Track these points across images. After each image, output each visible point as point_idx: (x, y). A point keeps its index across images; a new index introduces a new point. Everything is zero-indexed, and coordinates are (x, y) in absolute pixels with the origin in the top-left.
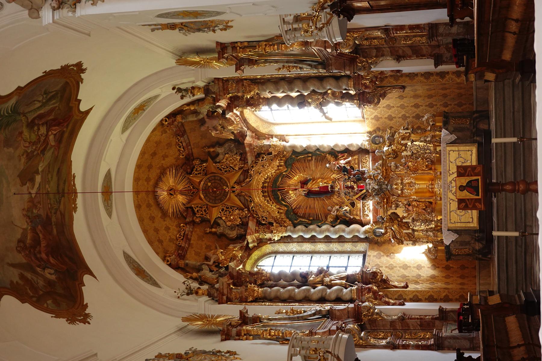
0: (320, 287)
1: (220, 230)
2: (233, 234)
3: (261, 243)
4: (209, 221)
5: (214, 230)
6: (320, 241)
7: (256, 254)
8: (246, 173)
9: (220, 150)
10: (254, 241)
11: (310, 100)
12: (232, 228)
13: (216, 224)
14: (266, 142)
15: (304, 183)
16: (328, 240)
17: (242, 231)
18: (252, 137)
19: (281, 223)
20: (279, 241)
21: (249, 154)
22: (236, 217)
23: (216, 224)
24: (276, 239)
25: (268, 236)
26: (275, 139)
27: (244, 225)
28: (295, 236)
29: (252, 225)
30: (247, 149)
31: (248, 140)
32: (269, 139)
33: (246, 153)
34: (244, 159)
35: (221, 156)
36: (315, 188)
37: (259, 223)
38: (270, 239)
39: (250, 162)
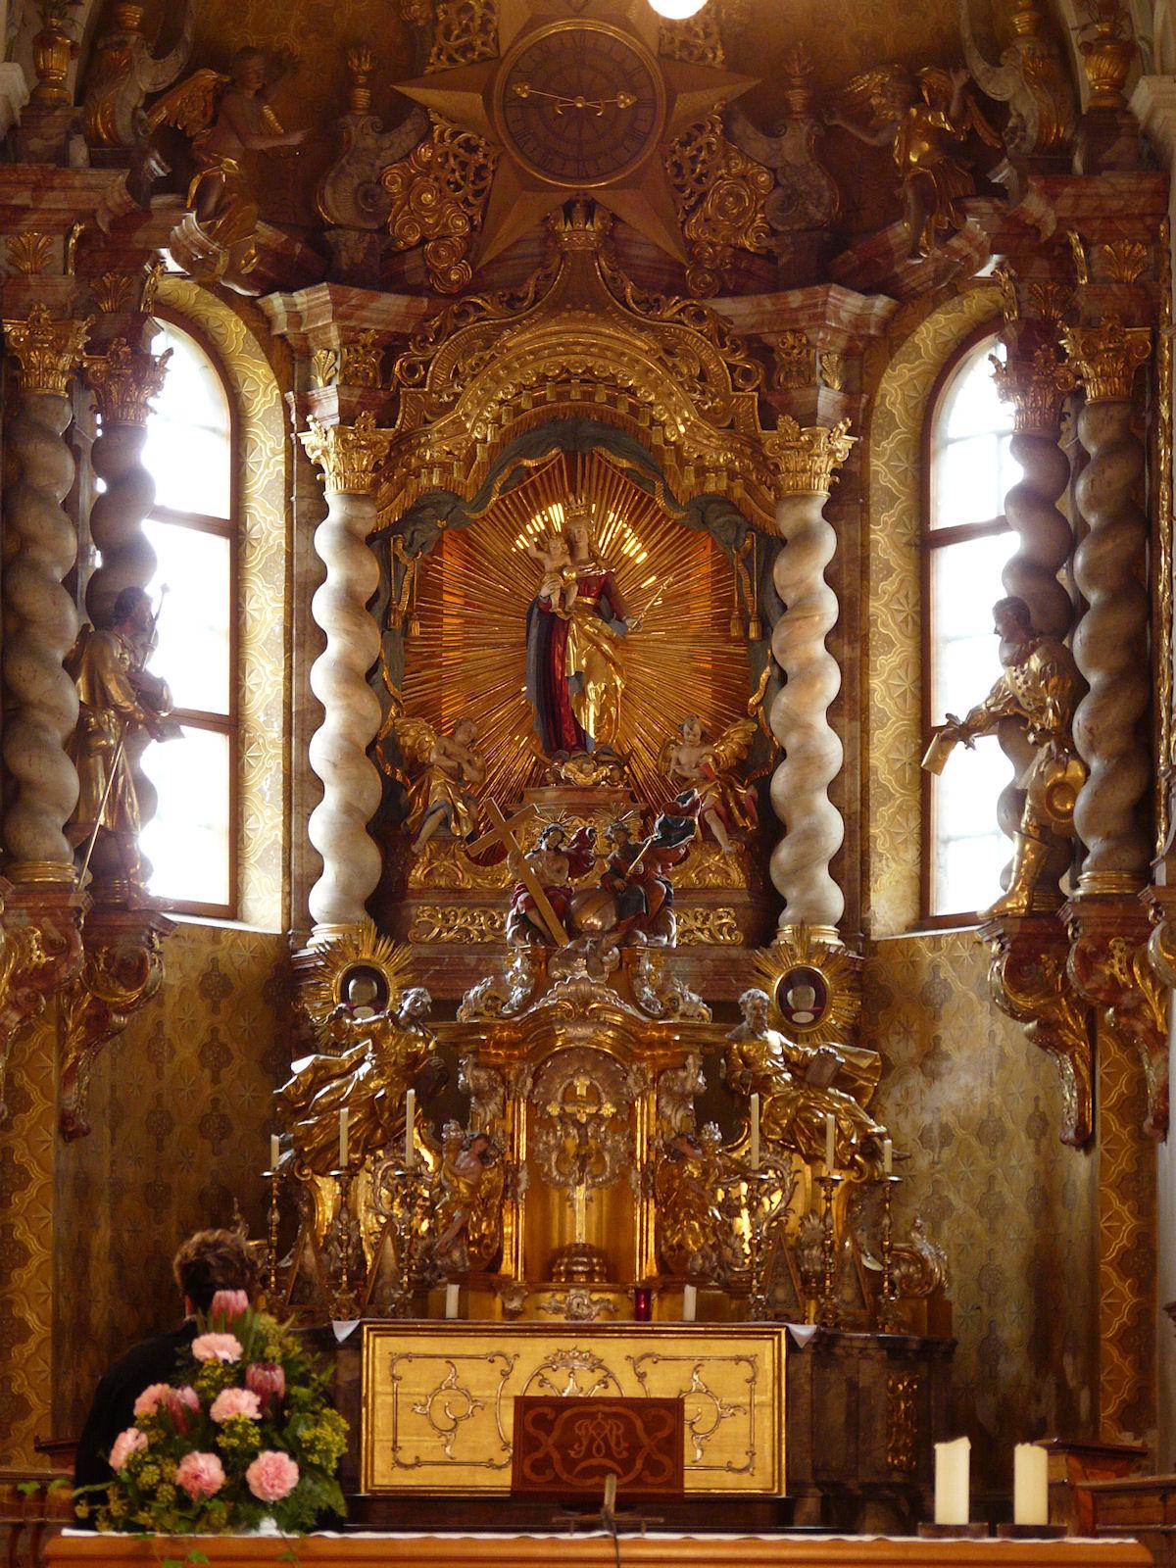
0: (74, 694)
1: (360, 130)
2: (337, 204)
3: (291, 362)
4: (413, 72)
5: (362, 96)
6: (295, 674)
7: (234, 330)
8: (667, 281)
9: (795, 143)
10: (295, 318)
11: (1035, 663)
12: (370, 194)
13: (393, 113)
14: (828, 398)
15: (606, 597)
16: (303, 717)
17: (352, 247)
18: (860, 321)
19: (387, 468)
20: (295, 452)
21: (767, 303)
22: (431, 215)
23: (393, 113)
24: (308, 439)
25: (328, 403)
26: (844, 444)
27: (384, 272)
28: (325, 540)
29: (390, 306)
30: (795, 298)
31: (848, 304)
32: (848, 411)
33: (777, 286)
34: (745, 274)
35: (760, 145)
36: (575, 658)
37: (391, 346)
38: (305, 407)
39: (725, 306)
